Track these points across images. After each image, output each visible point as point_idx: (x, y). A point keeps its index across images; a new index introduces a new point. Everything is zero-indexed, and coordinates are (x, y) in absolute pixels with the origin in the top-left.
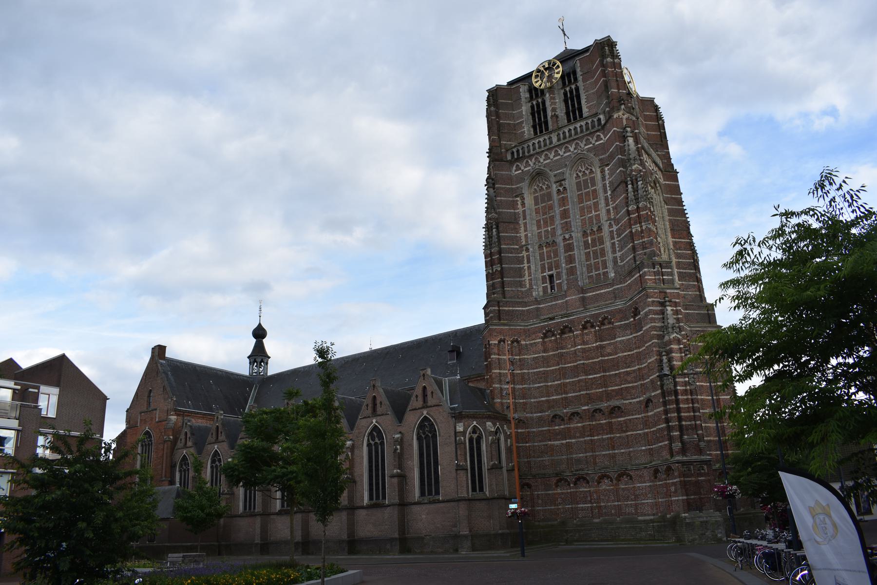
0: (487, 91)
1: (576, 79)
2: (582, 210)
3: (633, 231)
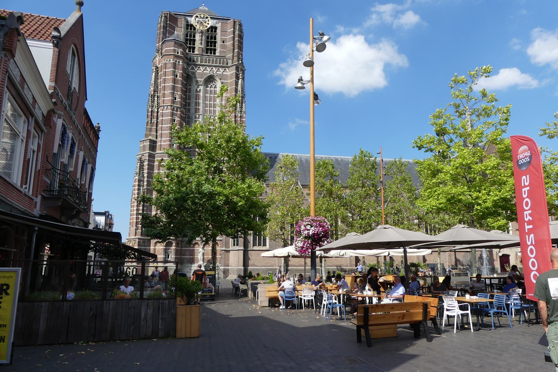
1: (215, 31)
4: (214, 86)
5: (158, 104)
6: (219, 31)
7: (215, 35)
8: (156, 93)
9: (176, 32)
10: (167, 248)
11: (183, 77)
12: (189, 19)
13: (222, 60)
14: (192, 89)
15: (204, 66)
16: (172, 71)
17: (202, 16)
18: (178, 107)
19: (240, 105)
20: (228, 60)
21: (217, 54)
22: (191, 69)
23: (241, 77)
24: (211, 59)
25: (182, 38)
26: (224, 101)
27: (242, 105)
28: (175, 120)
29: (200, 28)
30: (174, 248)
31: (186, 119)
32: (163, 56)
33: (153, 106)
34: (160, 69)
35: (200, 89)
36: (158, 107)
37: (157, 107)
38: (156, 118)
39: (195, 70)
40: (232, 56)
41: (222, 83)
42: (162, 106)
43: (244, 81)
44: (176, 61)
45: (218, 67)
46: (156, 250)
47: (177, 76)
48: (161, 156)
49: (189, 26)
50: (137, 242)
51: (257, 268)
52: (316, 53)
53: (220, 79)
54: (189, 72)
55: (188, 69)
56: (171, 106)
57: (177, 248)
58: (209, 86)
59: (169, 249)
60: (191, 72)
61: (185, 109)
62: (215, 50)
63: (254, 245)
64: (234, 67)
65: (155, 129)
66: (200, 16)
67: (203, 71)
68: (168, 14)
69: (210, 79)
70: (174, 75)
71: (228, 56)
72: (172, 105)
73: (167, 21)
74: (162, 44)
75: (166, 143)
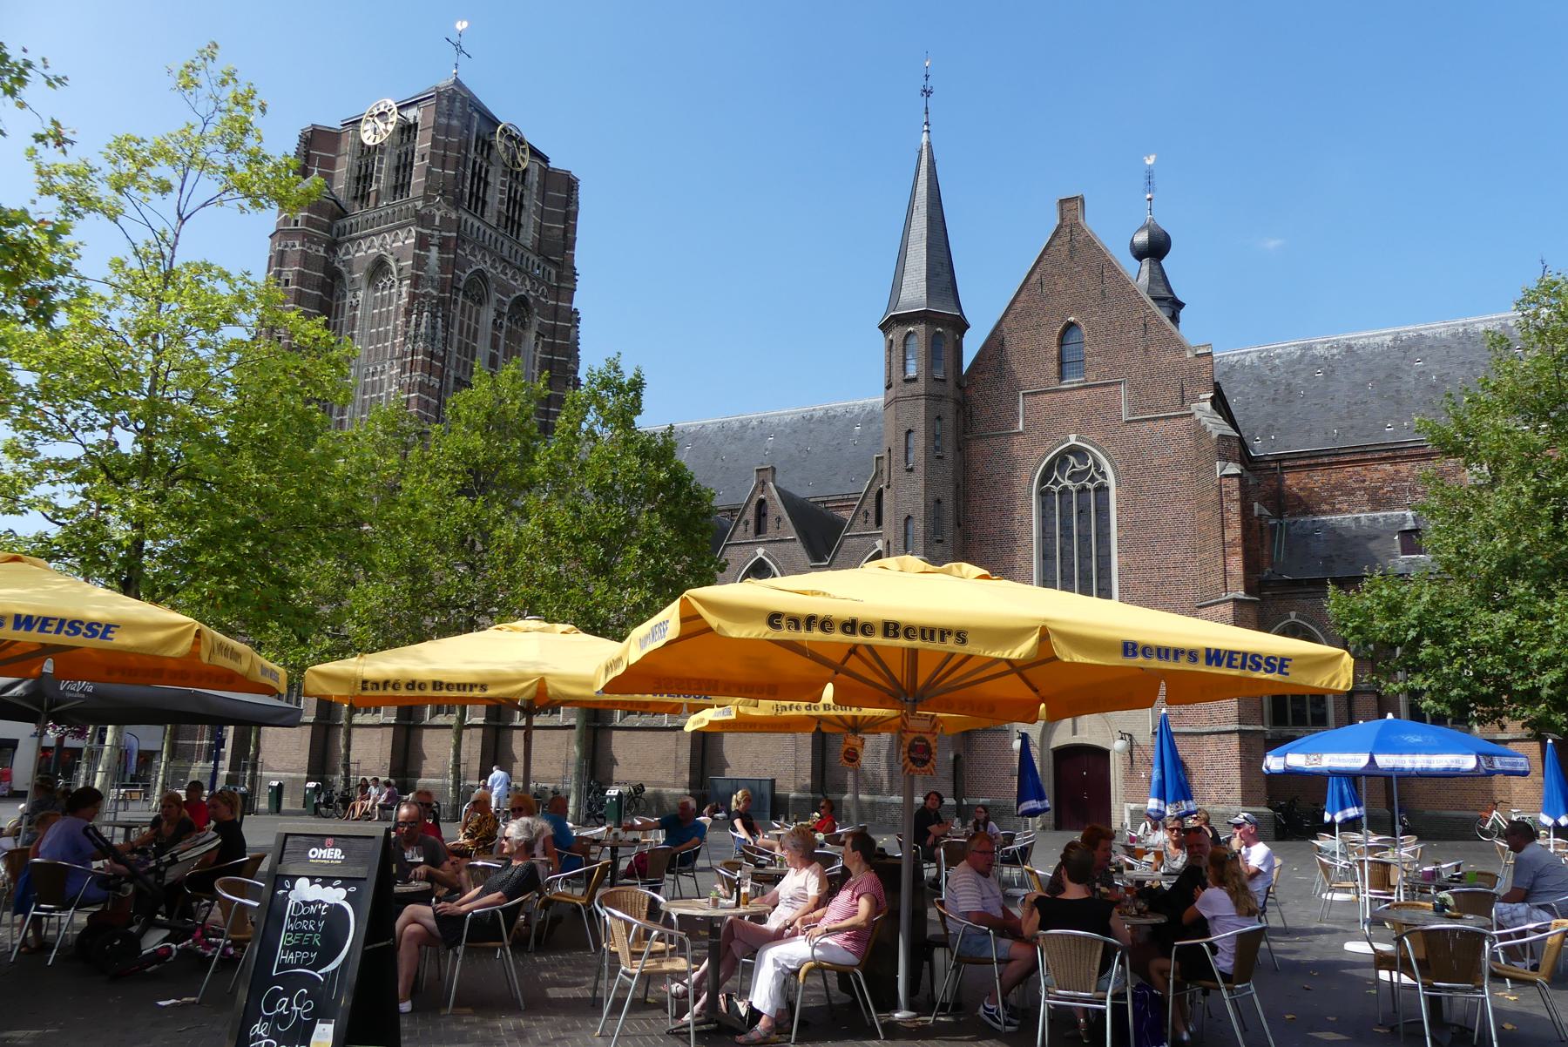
4: (389, 283)
45: (393, 230)
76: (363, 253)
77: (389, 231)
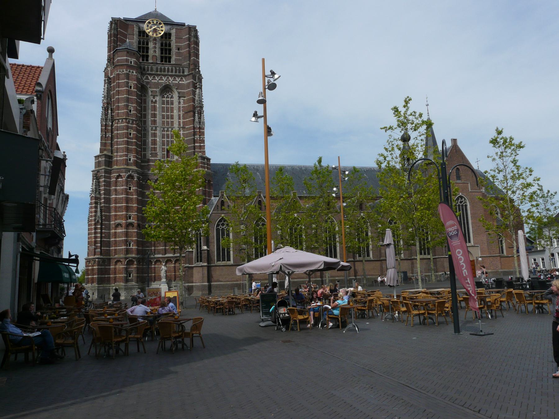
0: (112, 18)
1: (170, 38)
2: (163, 116)
3: (195, 138)
4: (170, 96)
5: (112, 118)
6: (173, 38)
7: (170, 42)
8: (110, 105)
9: (127, 40)
10: (128, 266)
11: (136, 87)
12: (141, 25)
13: (178, 68)
14: (147, 100)
15: (160, 75)
16: (125, 82)
17: (155, 22)
18: (134, 120)
19: (198, 116)
20: (184, 68)
21: (172, 63)
22: (145, 79)
23: (198, 86)
24: (166, 68)
25: (135, 47)
26: (181, 111)
27: (201, 116)
28: (130, 134)
29: (153, 35)
30: (135, 266)
31: (142, 131)
32: (115, 66)
33: (107, 120)
34: (112, 81)
35: (156, 100)
36: (112, 120)
37: (111, 121)
38: (110, 132)
39: (149, 79)
40: (188, 64)
41: (179, 93)
42: (116, 119)
43: (202, 90)
44: (130, 72)
46: (117, 269)
47: (131, 87)
48: (117, 172)
49: (142, 33)
50: (96, 262)
51: (222, 283)
52: (267, 90)
53: (177, 89)
54: (143, 82)
55: (142, 79)
56: (126, 119)
57: (138, 266)
58: (165, 96)
59: (129, 268)
60: (145, 82)
61: (141, 121)
62: (170, 58)
63: (218, 260)
64: (191, 76)
65: (110, 144)
66: (153, 22)
67: (158, 81)
68: (118, 20)
69: (166, 89)
70: (128, 86)
71: (183, 64)
72: (127, 117)
73: (118, 29)
74: (114, 53)
75: (122, 158)
76: (156, 81)
77: (171, 76)
